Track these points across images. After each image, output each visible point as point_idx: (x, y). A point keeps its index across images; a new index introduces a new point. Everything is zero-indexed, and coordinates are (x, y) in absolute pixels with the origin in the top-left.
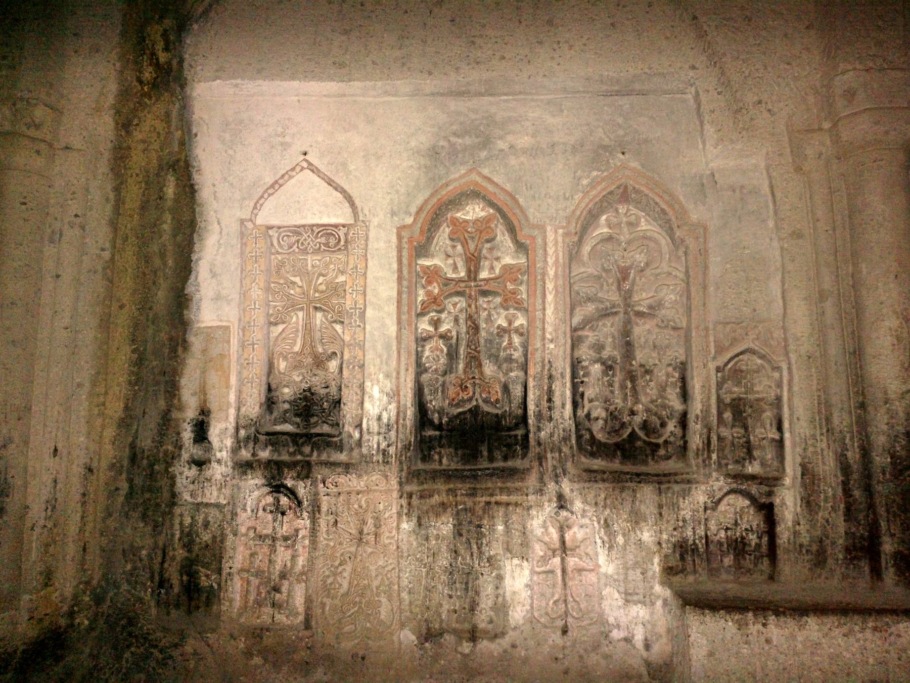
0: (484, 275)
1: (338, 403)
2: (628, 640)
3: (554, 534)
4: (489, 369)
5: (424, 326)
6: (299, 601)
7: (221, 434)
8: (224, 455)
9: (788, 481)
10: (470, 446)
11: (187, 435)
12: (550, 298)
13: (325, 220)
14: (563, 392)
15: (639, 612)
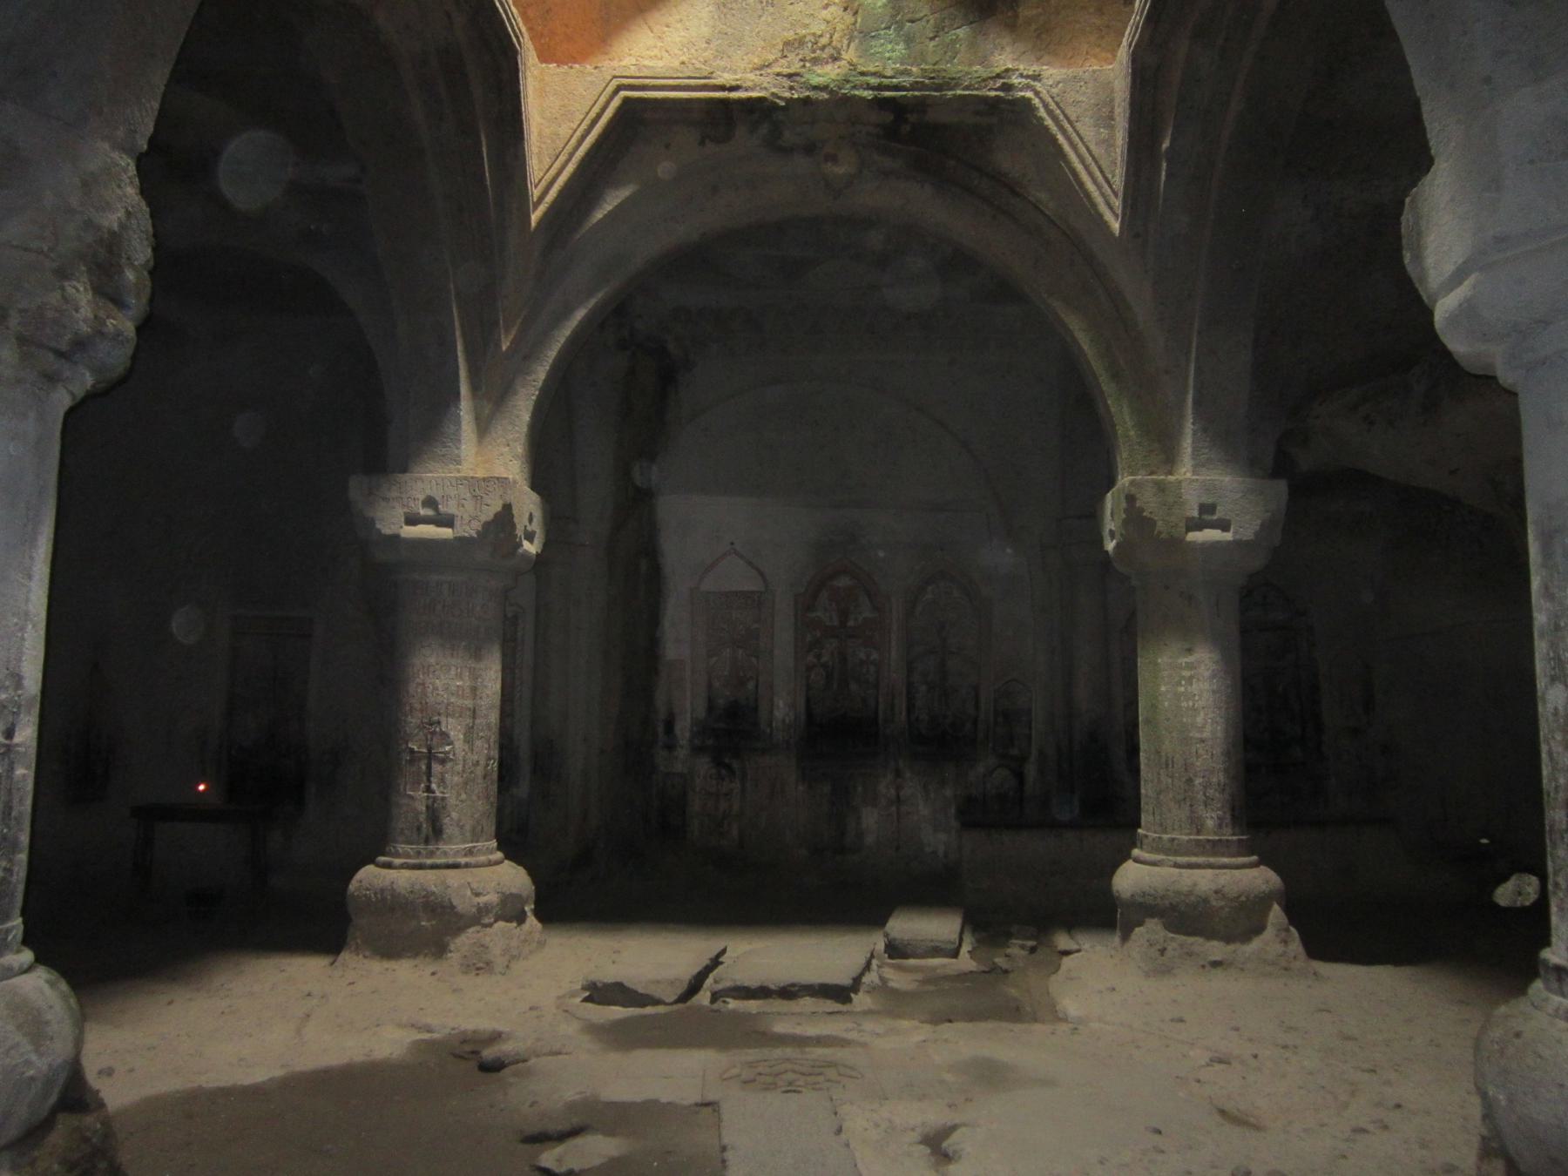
0: (851, 623)
1: (756, 709)
2: (934, 852)
3: (893, 791)
4: (853, 687)
5: (811, 658)
6: (735, 832)
7: (683, 729)
8: (684, 742)
9: (1032, 759)
10: (841, 736)
11: (661, 729)
12: (894, 643)
13: (746, 588)
14: (901, 704)
15: (942, 836)
